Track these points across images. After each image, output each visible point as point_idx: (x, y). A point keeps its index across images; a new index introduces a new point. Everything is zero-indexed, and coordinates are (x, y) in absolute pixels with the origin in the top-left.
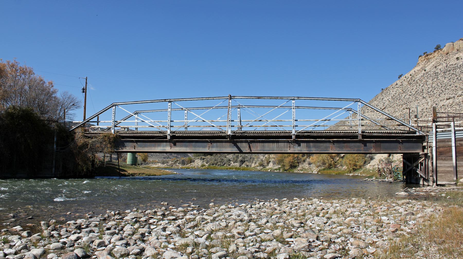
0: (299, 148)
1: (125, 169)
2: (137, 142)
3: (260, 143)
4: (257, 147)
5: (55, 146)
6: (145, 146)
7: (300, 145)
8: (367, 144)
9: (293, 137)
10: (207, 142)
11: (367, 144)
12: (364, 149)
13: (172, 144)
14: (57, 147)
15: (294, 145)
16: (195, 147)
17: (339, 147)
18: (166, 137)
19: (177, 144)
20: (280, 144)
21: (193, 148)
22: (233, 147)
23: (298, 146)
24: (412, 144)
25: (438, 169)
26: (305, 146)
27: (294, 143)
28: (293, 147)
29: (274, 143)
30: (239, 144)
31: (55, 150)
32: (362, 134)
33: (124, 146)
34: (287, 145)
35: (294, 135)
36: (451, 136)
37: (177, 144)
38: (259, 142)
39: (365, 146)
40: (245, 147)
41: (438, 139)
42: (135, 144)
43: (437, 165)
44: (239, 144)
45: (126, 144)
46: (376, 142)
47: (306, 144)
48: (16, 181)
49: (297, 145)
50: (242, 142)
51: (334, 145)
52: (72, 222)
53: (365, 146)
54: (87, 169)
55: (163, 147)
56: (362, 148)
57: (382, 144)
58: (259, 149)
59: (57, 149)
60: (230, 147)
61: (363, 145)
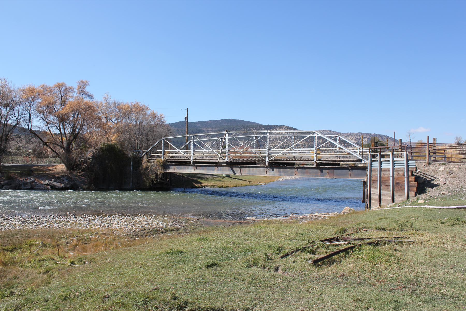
0: (273, 173)
1: (200, 181)
2: (176, 165)
3: (247, 168)
4: (245, 171)
5: (132, 168)
6: (181, 169)
7: (273, 170)
8: (323, 170)
9: (267, 164)
10: (214, 166)
11: (323, 170)
12: (321, 174)
13: (195, 168)
14: (133, 168)
15: (269, 170)
16: (208, 170)
17: (302, 173)
18: (190, 162)
19: (198, 167)
20: (260, 169)
21: (207, 171)
22: (230, 171)
23: (272, 171)
24: (360, 171)
25: (372, 197)
26: (277, 171)
27: (269, 168)
28: (269, 172)
29: (256, 168)
30: (234, 168)
31: (132, 171)
32: (316, 162)
33: (169, 168)
34: (265, 170)
35: (267, 162)
36: (404, 163)
37: (198, 167)
38: (247, 167)
39: (322, 172)
40: (238, 171)
41: (373, 168)
42: (175, 167)
43: (372, 193)
44: (234, 168)
45: (171, 167)
46: (330, 168)
47: (278, 170)
48: (89, 193)
49: (271, 170)
50: (235, 167)
51: (298, 170)
52: (49, 224)
53: (322, 172)
54: (149, 184)
55: (190, 169)
56: (319, 174)
57: (335, 171)
58: (246, 172)
59: (133, 170)
60: (229, 170)
61: (320, 171)
